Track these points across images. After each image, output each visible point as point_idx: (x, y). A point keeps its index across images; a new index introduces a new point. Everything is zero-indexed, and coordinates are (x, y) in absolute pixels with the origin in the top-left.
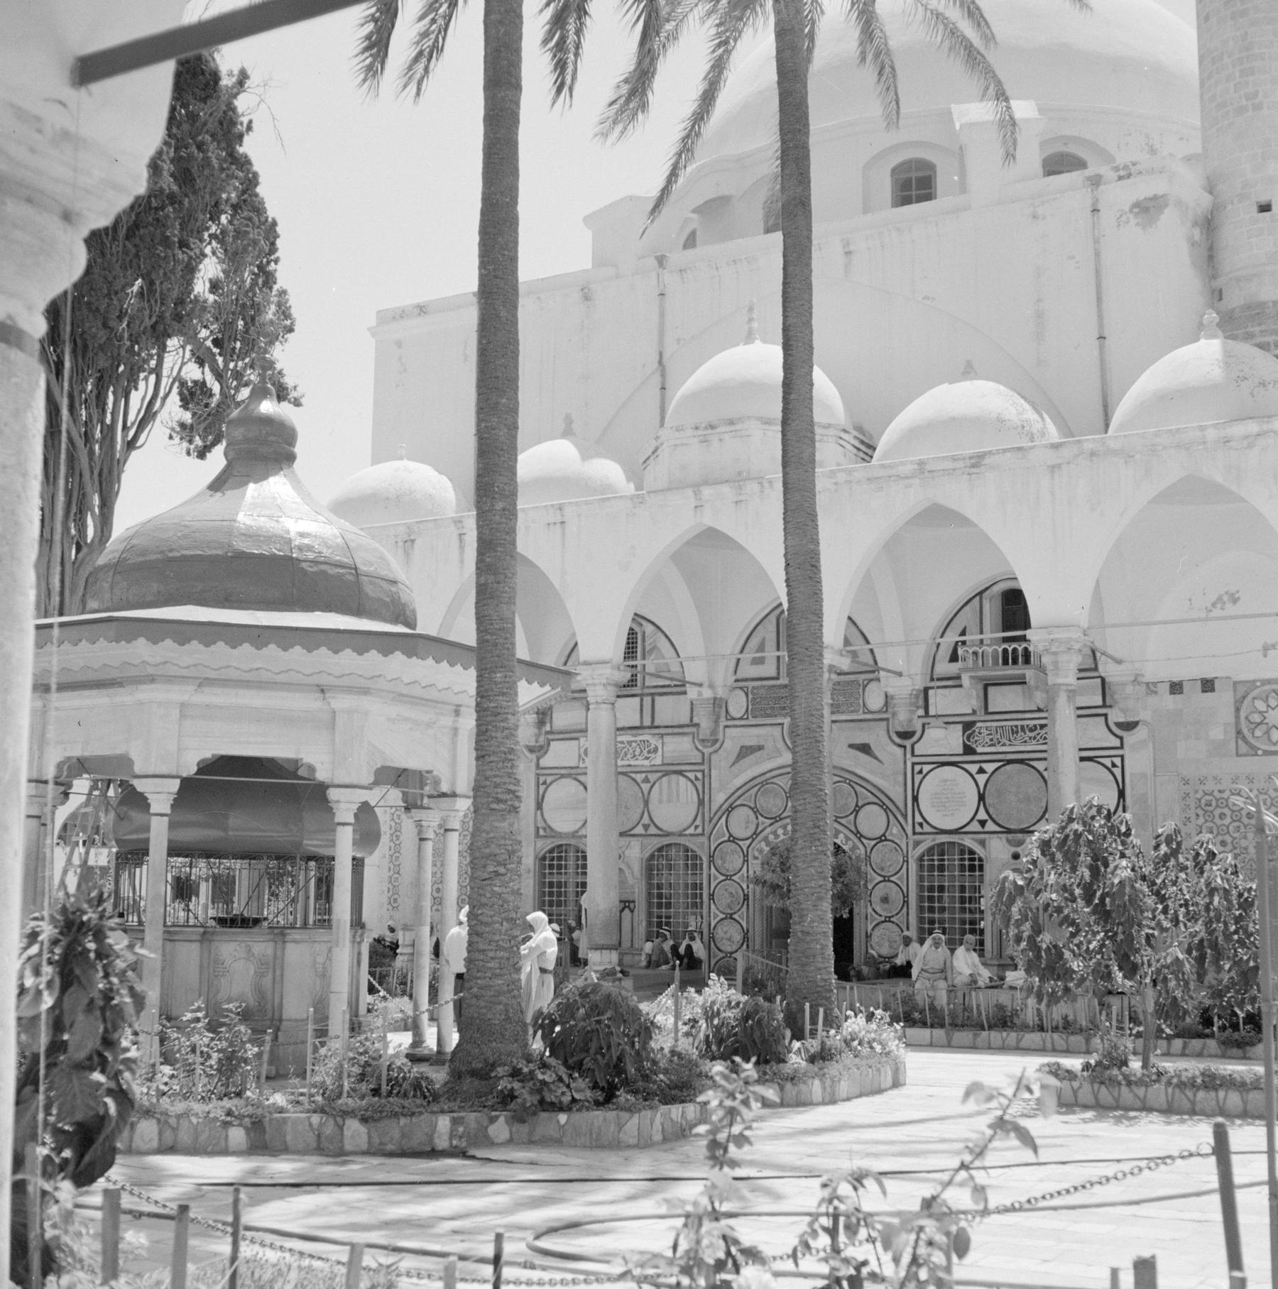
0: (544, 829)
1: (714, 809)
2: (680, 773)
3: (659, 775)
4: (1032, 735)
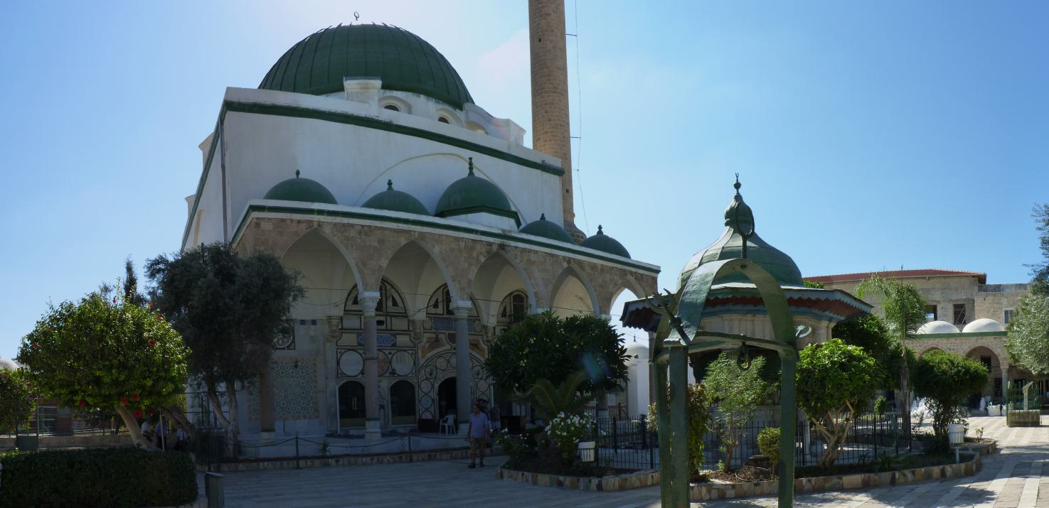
2: (405, 351)
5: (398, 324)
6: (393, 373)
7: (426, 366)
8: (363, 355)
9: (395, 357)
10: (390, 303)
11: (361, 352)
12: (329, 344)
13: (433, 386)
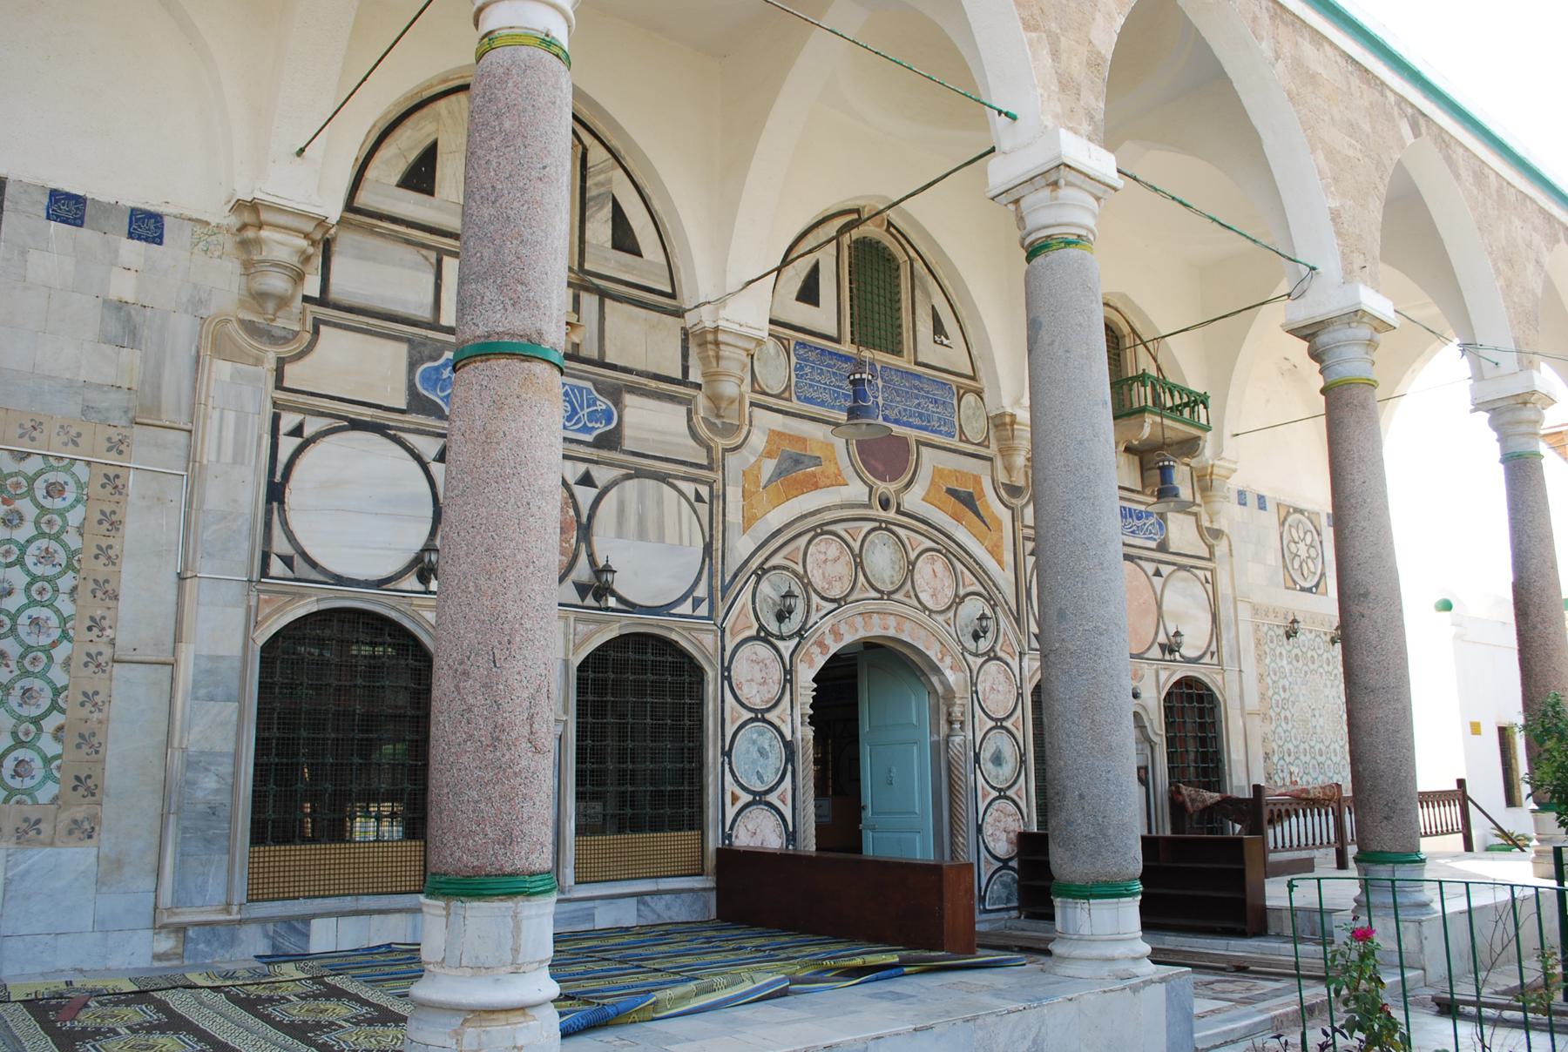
0: (287, 561)
1: (732, 566)
2: (663, 478)
3: (617, 473)
4: (1139, 523)
5: (638, 340)
6: (598, 588)
7: (761, 573)
8: (437, 469)
9: (613, 493)
10: (600, 230)
11: (429, 447)
12: (222, 370)
13: (789, 675)
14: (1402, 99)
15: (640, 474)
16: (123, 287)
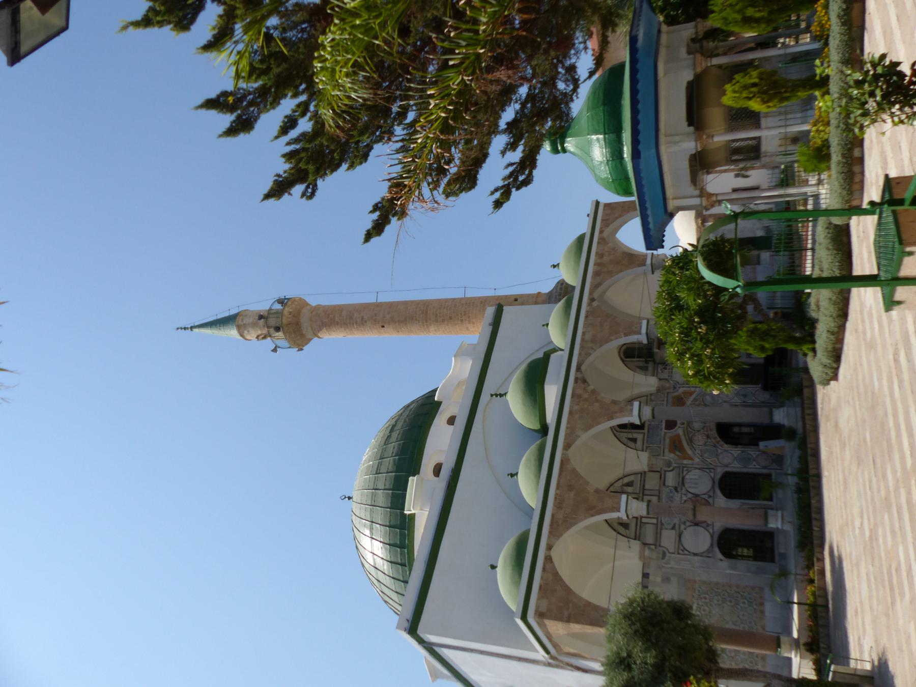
2: (683, 478)
10: (630, 489)
14: (589, 304)
15: (683, 483)
16: (659, 579)
